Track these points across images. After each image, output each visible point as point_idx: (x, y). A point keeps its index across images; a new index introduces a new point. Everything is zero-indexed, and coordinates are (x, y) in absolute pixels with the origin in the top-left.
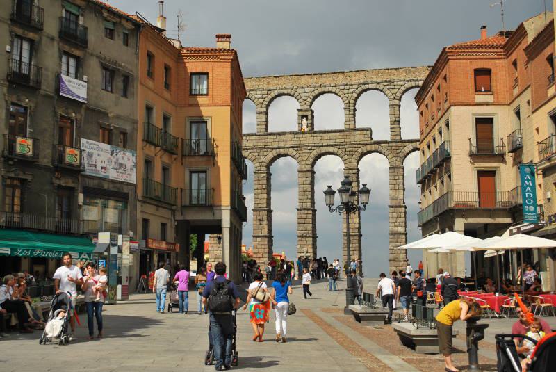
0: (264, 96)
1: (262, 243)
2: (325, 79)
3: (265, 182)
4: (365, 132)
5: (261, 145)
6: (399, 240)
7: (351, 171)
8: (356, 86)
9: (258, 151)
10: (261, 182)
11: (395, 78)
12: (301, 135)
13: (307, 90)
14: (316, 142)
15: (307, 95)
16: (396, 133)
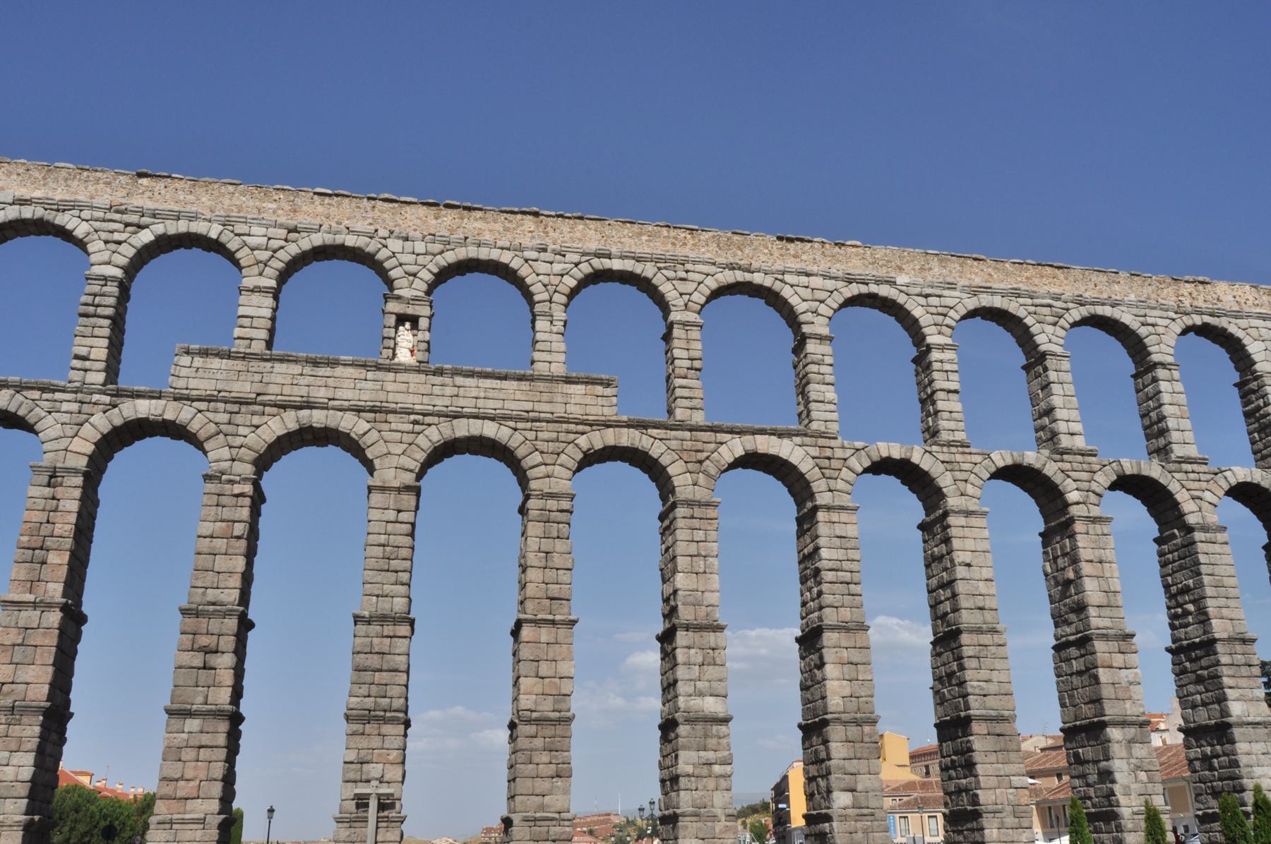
0: (275, 244)
1: (205, 739)
2: (479, 225)
3: (245, 513)
4: (599, 390)
5: (244, 388)
6: (712, 742)
7: (552, 504)
8: (576, 258)
9: (230, 407)
10: (227, 513)
11: (681, 252)
12: (391, 376)
13: (420, 247)
14: (439, 401)
15: (421, 259)
16: (695, 403)
